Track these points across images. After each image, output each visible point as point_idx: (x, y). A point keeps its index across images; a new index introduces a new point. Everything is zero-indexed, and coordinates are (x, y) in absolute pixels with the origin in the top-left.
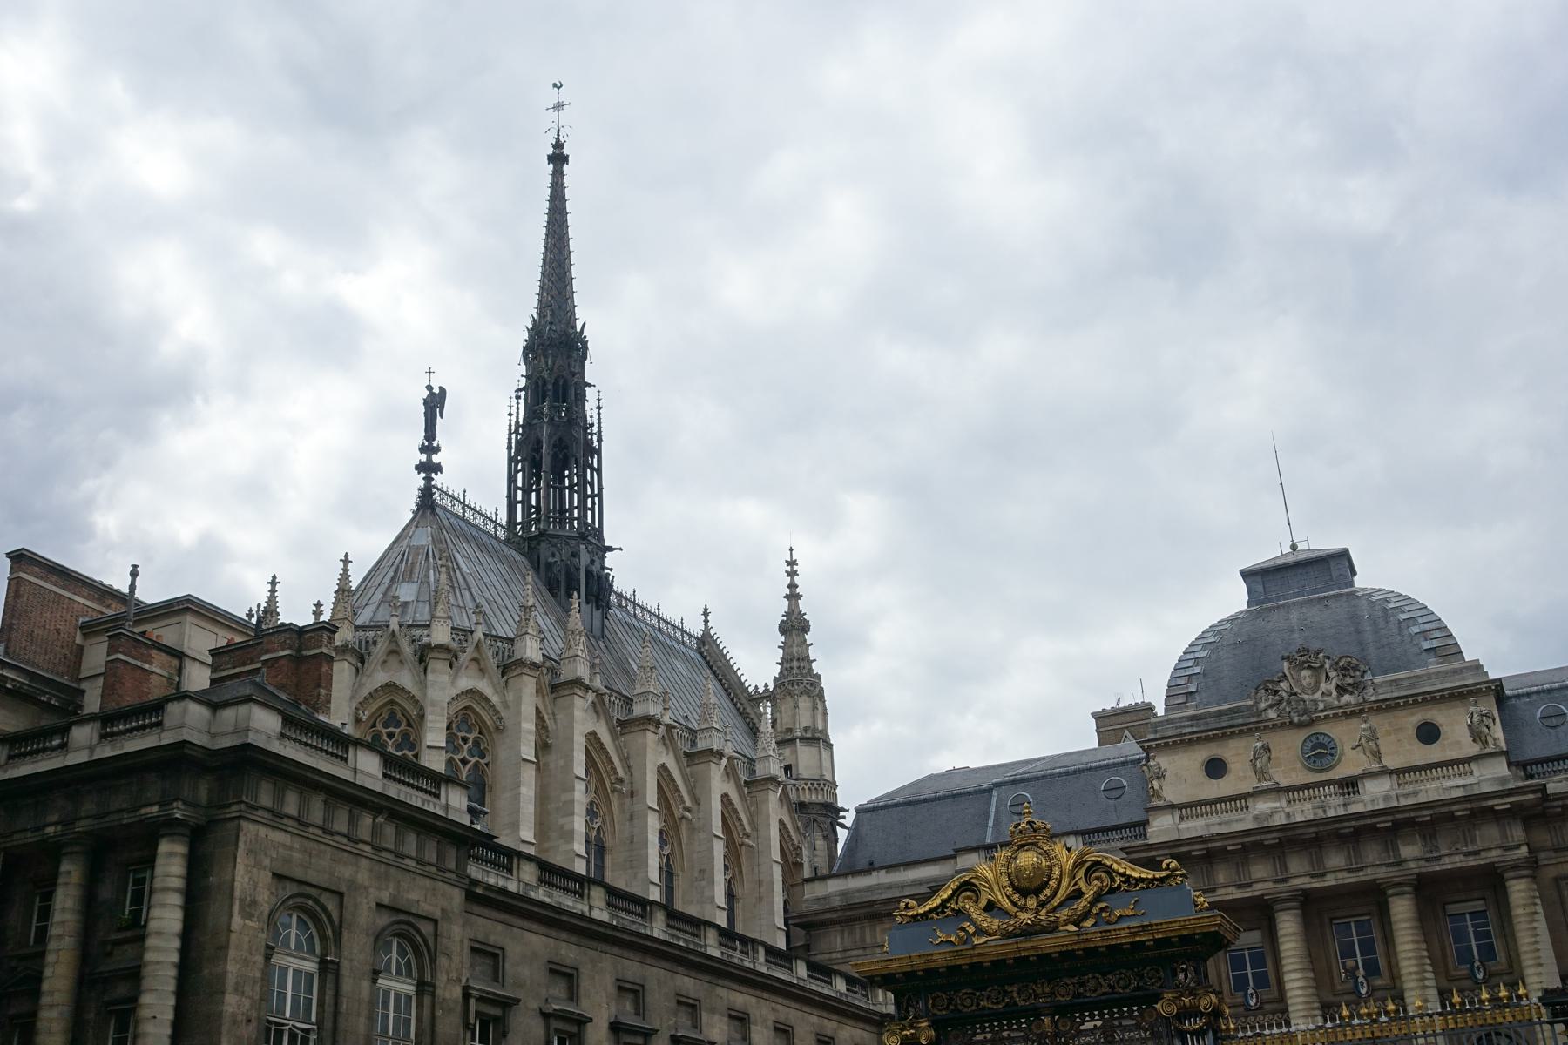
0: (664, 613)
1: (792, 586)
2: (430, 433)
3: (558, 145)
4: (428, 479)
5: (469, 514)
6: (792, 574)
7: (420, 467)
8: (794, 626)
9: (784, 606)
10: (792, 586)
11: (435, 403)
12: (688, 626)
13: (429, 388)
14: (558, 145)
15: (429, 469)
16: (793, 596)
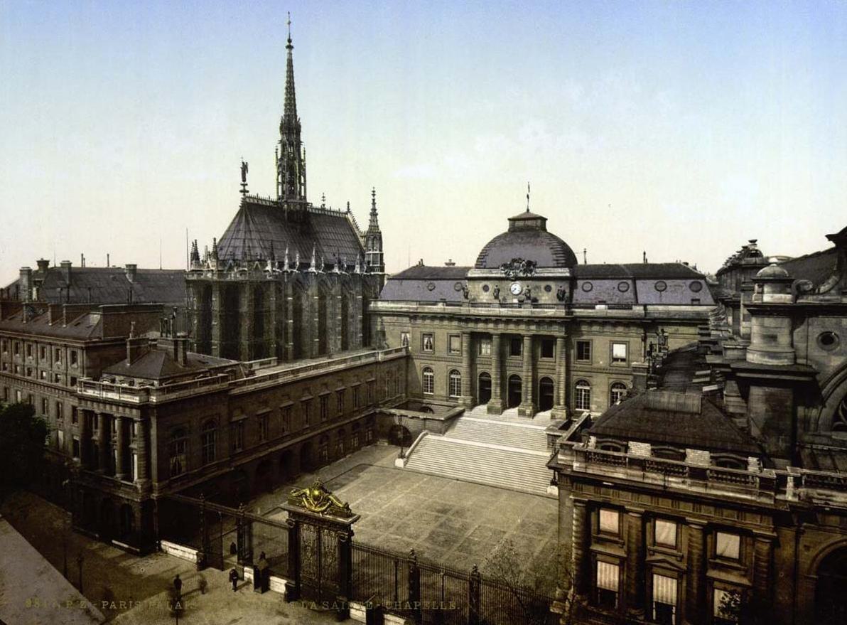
0: (333, 209)
1: (374, 200)
2: (244, 179)
3: (290, 41)
4: (244, 195)
5: (260, 202)
6: (374, 195)
7: (241, 191)
8: (374, 214)
9: (371, 207)
10: (374, 200)
11: (245, 168)
12: (341, 210)
13: (243, 163)
14: (290, 41)
15: (244, 191)
16: (374, 204)
